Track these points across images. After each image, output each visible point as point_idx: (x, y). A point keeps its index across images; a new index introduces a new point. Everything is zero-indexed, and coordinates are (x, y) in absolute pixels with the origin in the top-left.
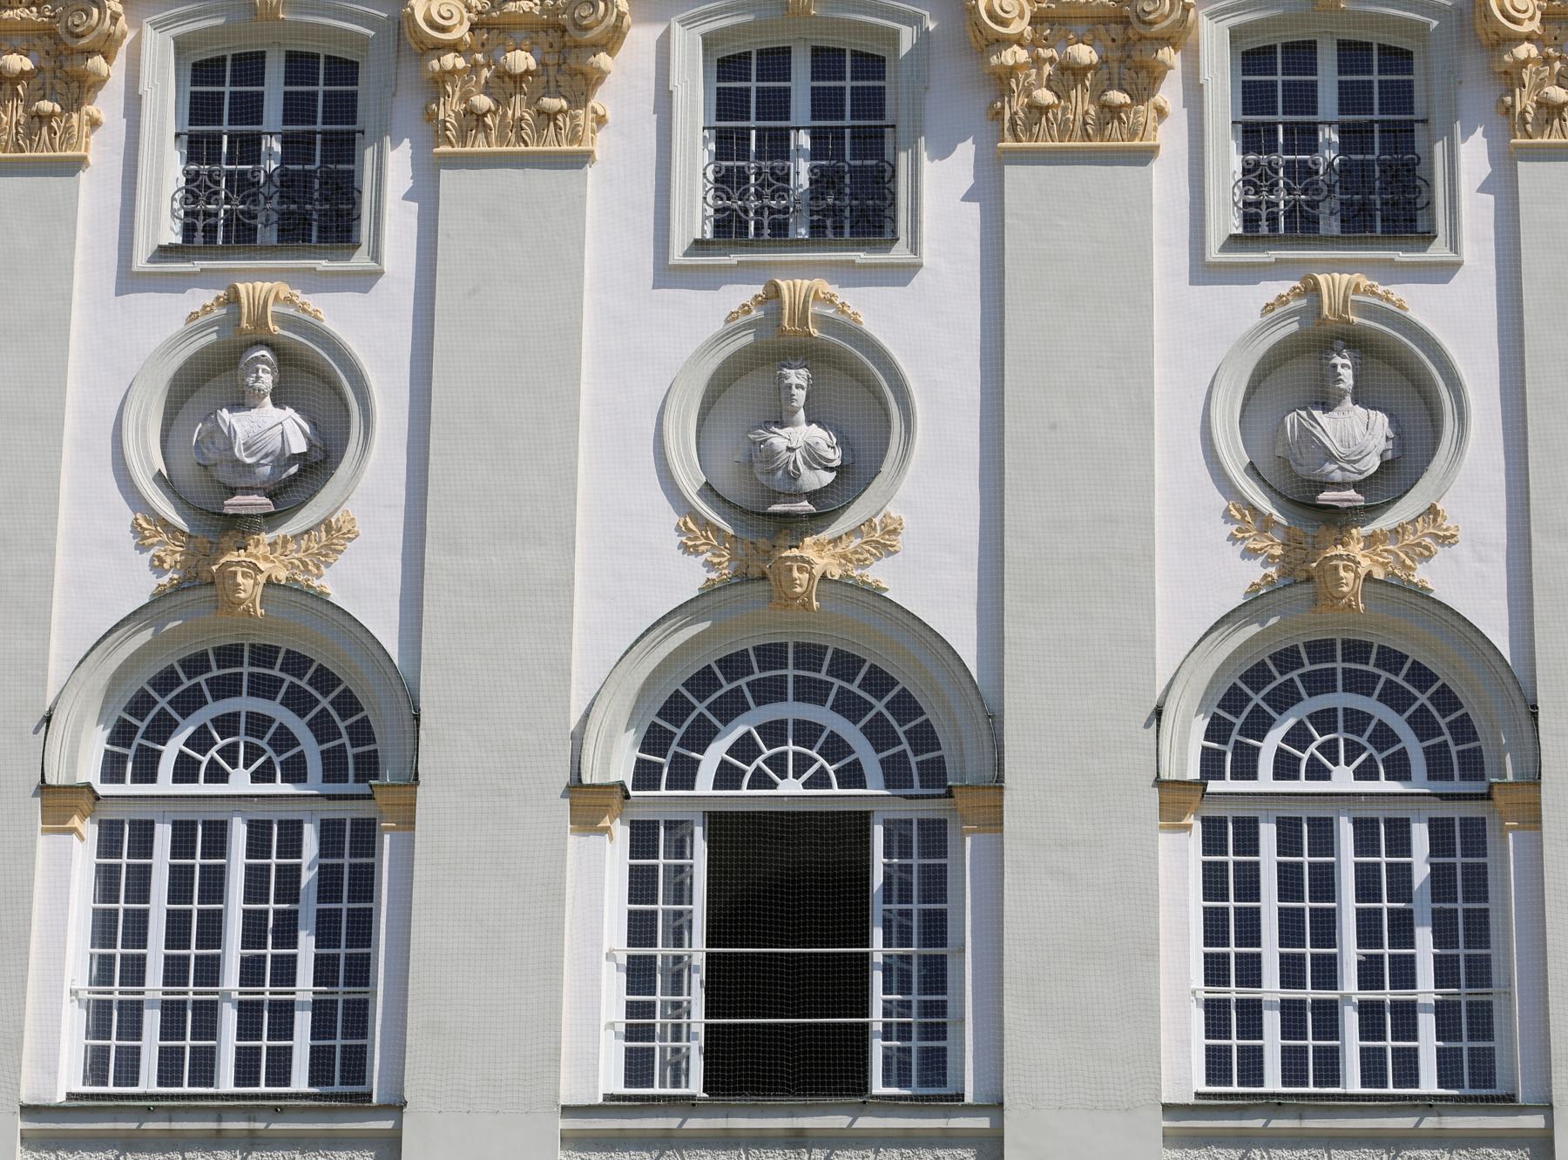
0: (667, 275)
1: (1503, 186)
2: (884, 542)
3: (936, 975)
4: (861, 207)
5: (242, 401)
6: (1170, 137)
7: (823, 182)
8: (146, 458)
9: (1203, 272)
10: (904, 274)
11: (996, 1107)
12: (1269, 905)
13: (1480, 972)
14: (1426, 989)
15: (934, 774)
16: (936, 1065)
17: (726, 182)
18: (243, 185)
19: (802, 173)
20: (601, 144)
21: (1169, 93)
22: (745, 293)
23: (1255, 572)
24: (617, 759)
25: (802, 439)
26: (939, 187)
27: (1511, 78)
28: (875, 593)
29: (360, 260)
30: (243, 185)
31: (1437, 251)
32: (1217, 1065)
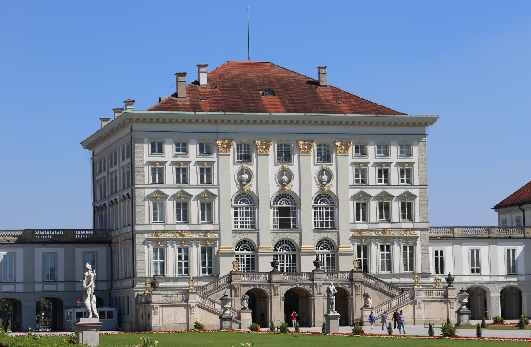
0: (275, 164)
1: (336, 158)
2: (292, 186)
3: (295, 219)
4: (288, 158)
5: (243, 174)
6: (312, 153)
7: (285, 156)
8: (237, 180)
9: (315, 165)
10: (292, 165)
11: (301, 230)
12: (319, 214)
13: (333, 219)
14: (330, 220)
15: (295, 204)
16: (296, 226)
17: (278, 156)
18: (241, 155)
19: (284, 155)
20: (270, 153)
21: (312, 150)
22: (281, 166)
23: (319, 189)
24: (272, 204)
25: (285, 178)
26: (295, 157)
27: (337, 150)
28: (291, 190)
29: (252, 163)
30: (241, 155)
31: (332, 163)
32: (315, 226)
